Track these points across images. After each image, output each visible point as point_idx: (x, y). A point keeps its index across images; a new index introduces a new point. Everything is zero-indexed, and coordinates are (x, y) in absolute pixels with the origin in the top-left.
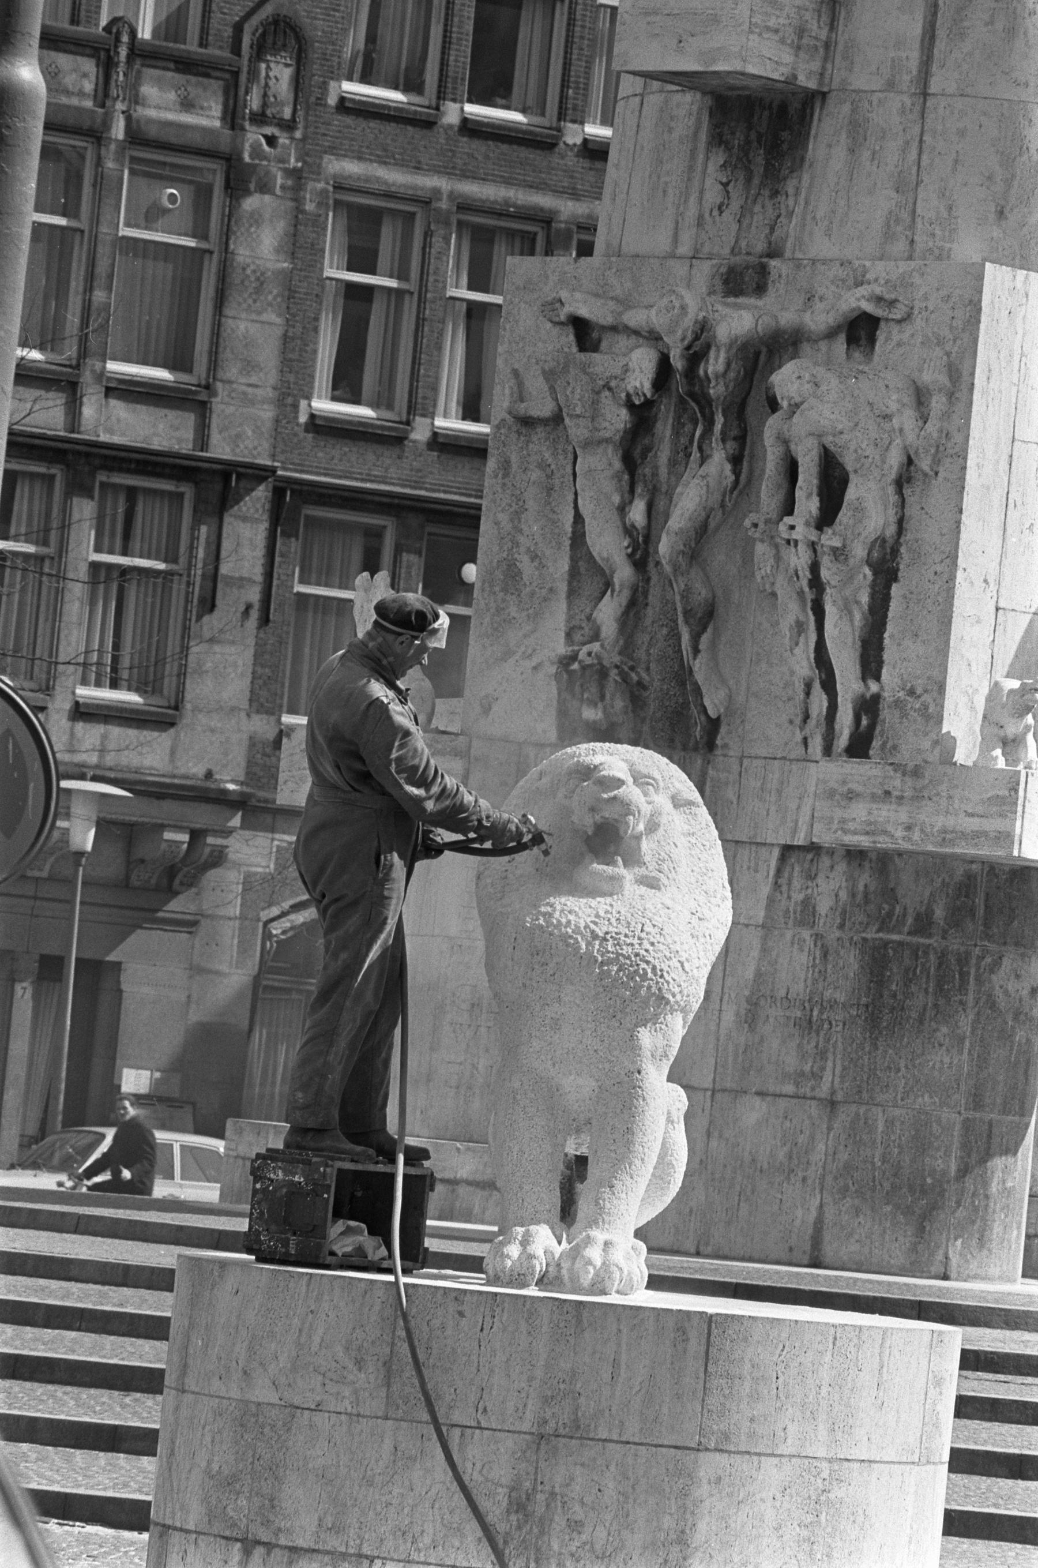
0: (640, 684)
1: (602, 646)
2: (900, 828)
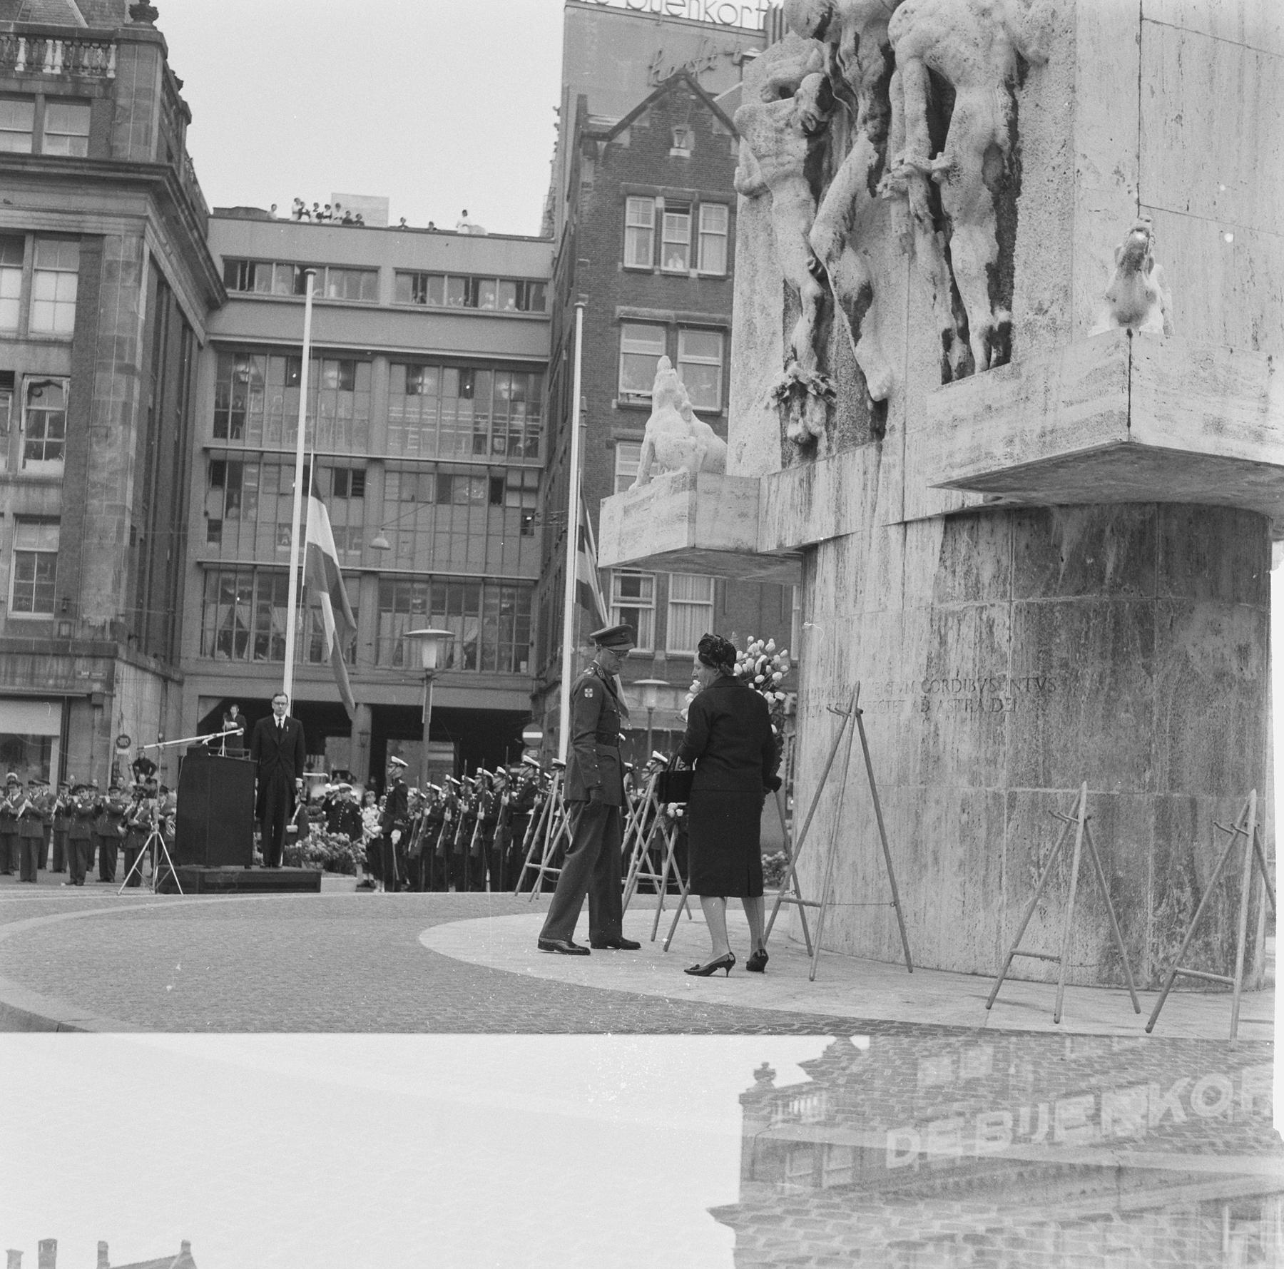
0: (829, 392)
1: (799, 365)
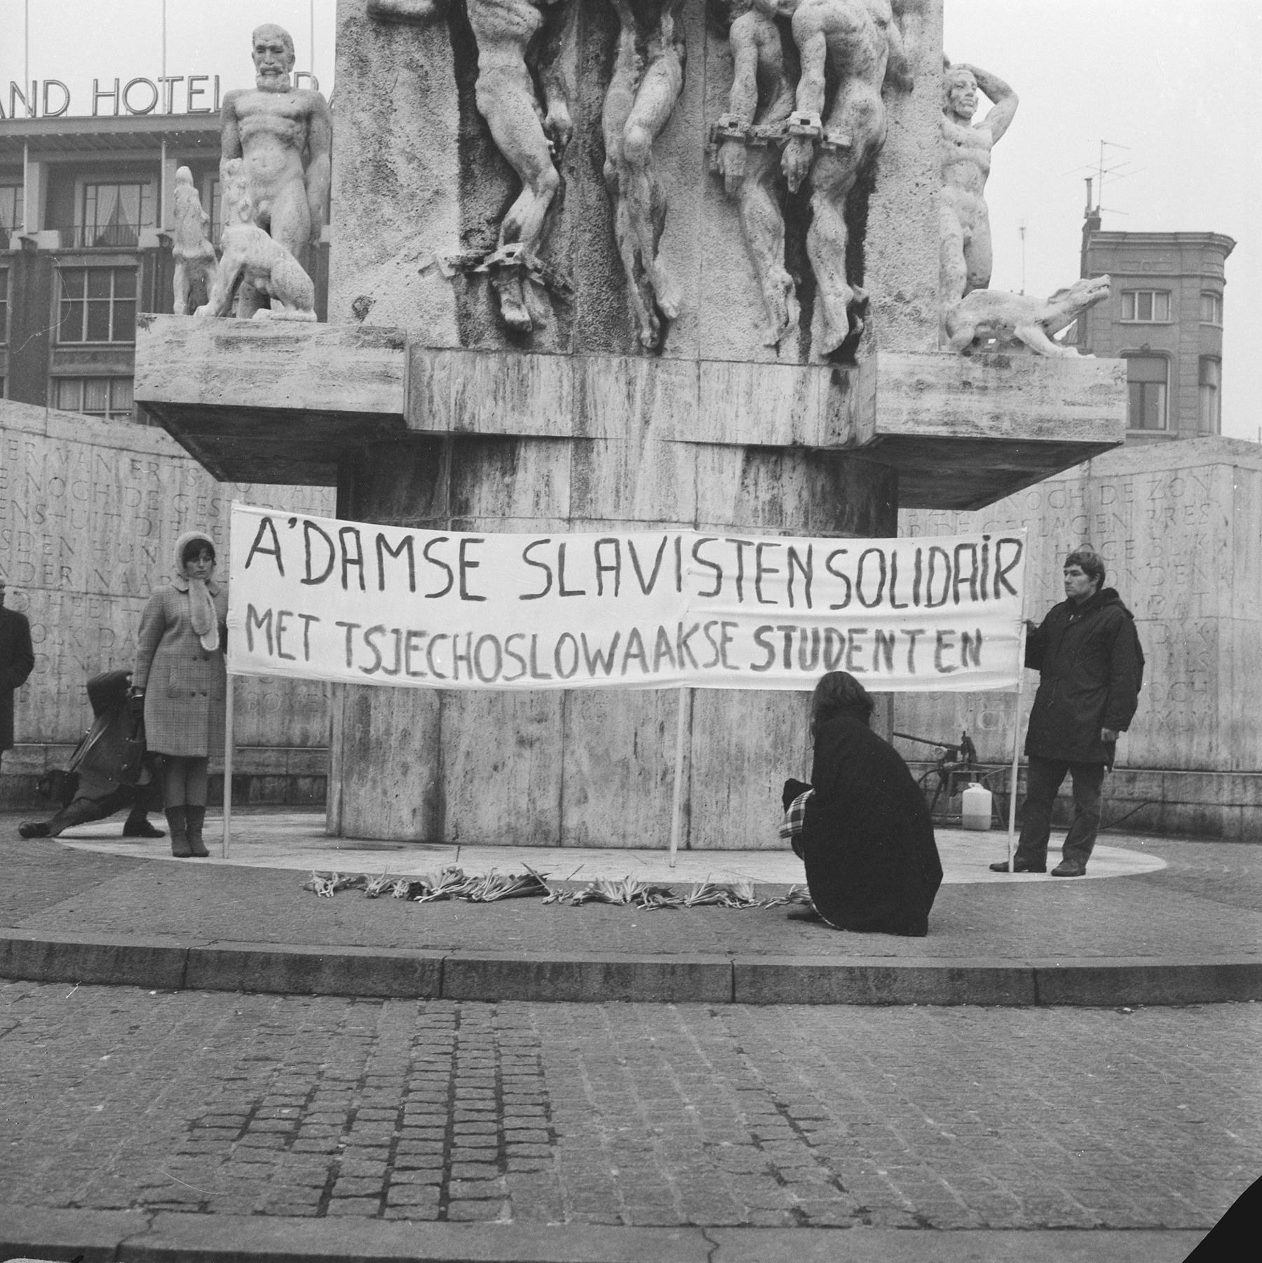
0: (566, 288)
2: (985, 418)
